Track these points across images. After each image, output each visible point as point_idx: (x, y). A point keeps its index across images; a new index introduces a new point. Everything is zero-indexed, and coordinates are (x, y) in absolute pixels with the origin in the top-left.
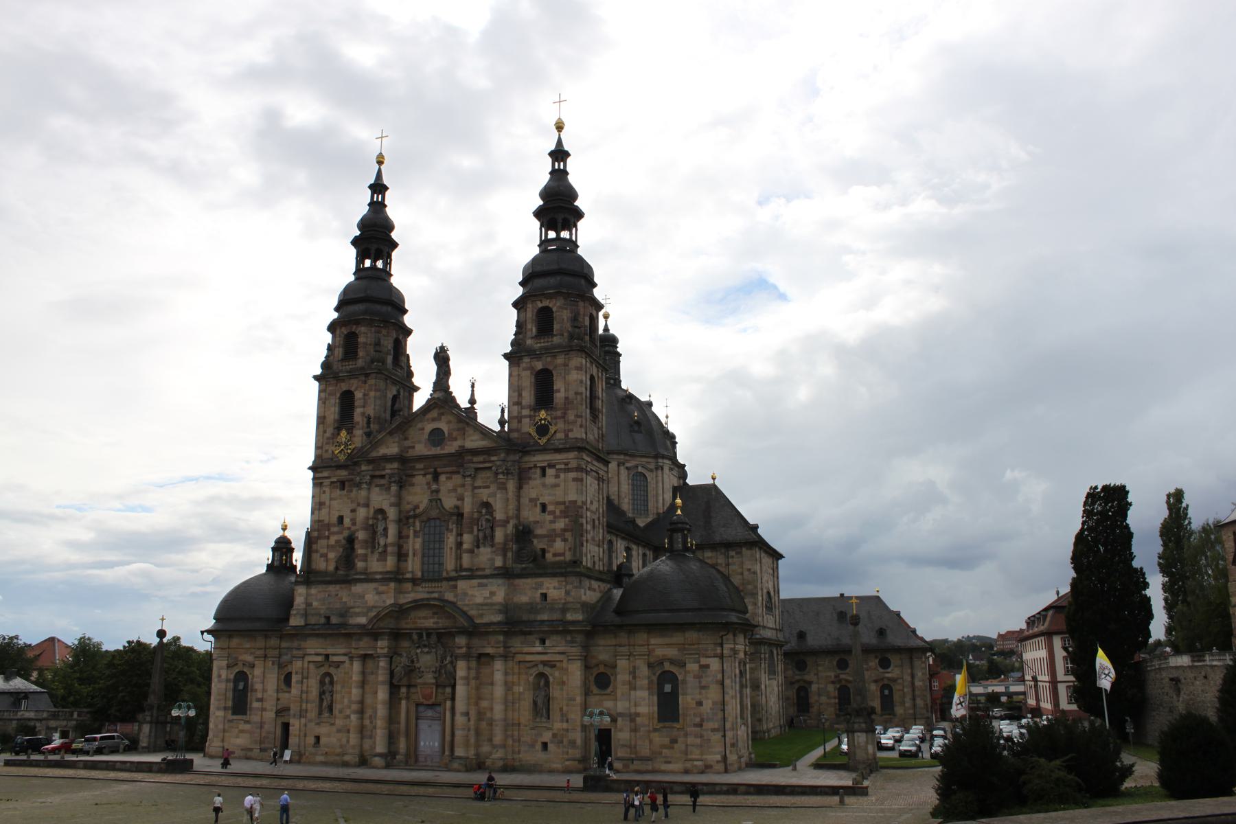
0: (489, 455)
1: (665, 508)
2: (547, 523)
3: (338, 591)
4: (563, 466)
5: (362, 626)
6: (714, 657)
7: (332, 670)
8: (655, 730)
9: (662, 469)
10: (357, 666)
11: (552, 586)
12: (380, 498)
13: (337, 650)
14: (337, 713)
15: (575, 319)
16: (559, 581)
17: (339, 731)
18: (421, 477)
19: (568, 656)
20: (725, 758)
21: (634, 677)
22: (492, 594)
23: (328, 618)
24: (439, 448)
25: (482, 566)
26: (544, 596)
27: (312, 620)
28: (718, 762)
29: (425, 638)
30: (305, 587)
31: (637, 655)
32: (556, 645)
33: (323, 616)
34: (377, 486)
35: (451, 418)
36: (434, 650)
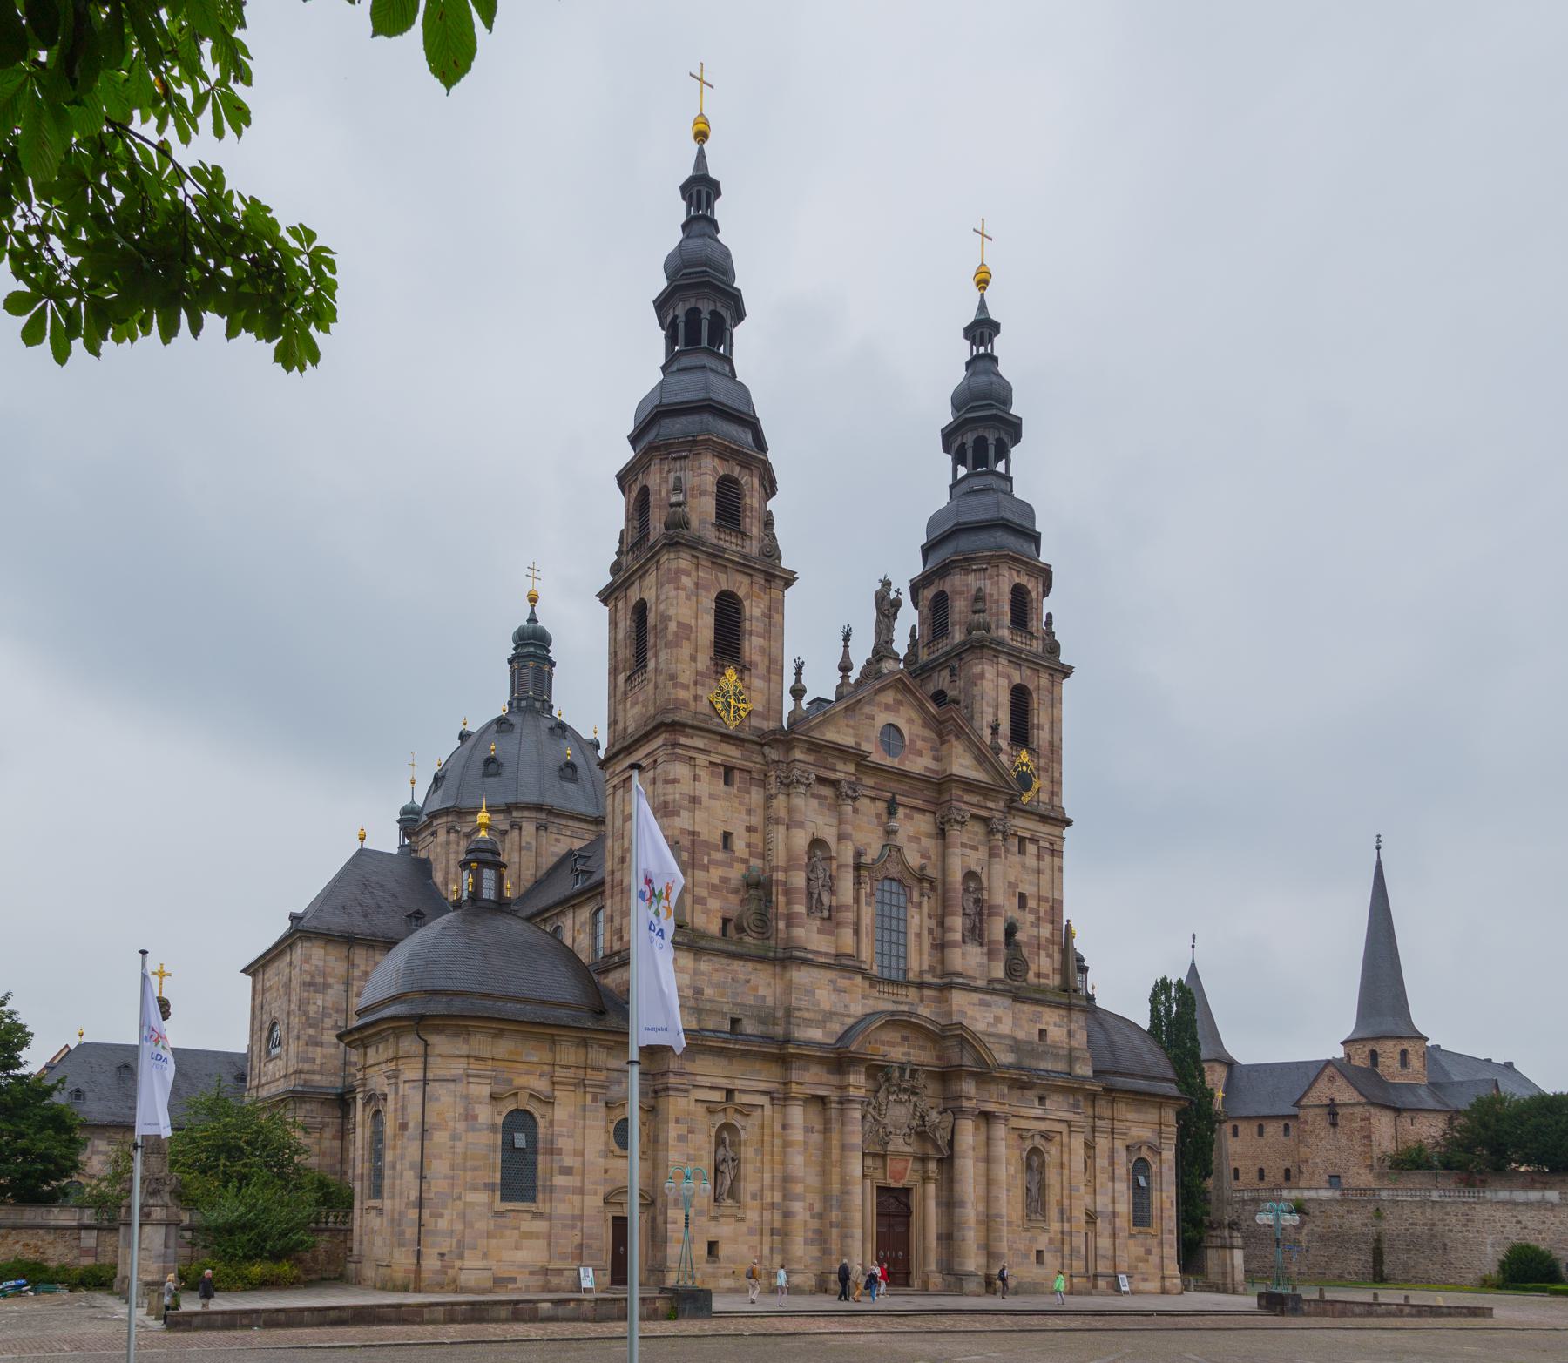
0: (985, 797)
2: (1028, 924)
3: (750, 973)
4: (1047, 845)
5: (821, 1045)
7: (737, 1120)
8: (1132, 1236)
10: (797, 1114)
11: (1051, 1021)
12: (820, 820)
13: (754, 1081)
14: (748, 1198)
16: (1059, 1015)
17: (751, 1232)
18: (867, 801)
19: (1070, 1126)
21: (1112, 1163)
22: (998, 1019)
23: (735, 1022)
24: (896, 760)
25: (971, 973)
26: (1042, 1033)
27: (710, 1023)
29: (907, 1077)
30: (692, 955)
31: (1118, 1133)
32: (1058, 1108)
33: (729, 1016)
34: (814, 796)
35: (914, 715)
36: (914, 1099)
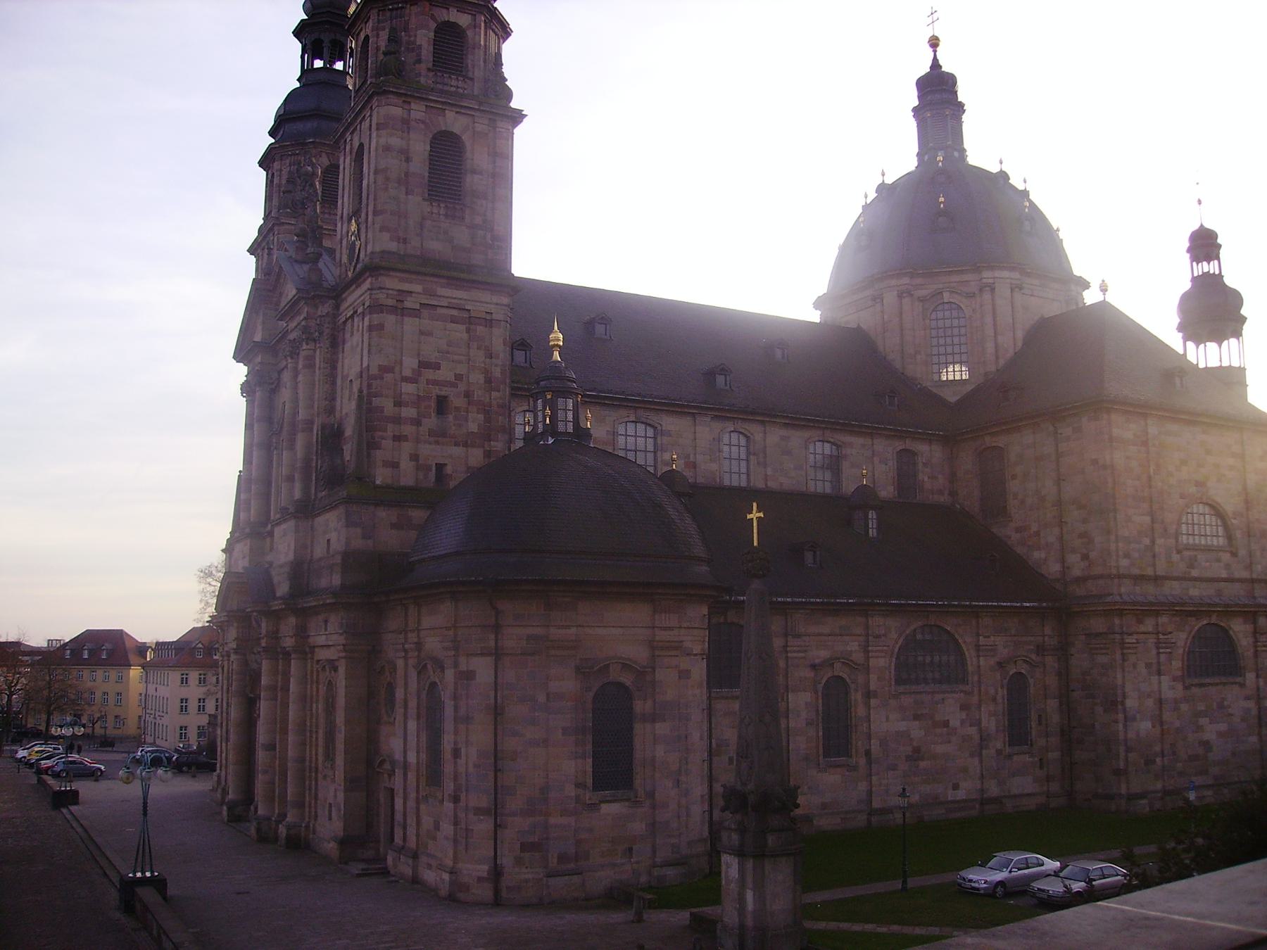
1: (1002, 362)
6: (482, 654)
9: (993, 290)
15: (393, 39)
20: (497, 873)
28: (480, 879)
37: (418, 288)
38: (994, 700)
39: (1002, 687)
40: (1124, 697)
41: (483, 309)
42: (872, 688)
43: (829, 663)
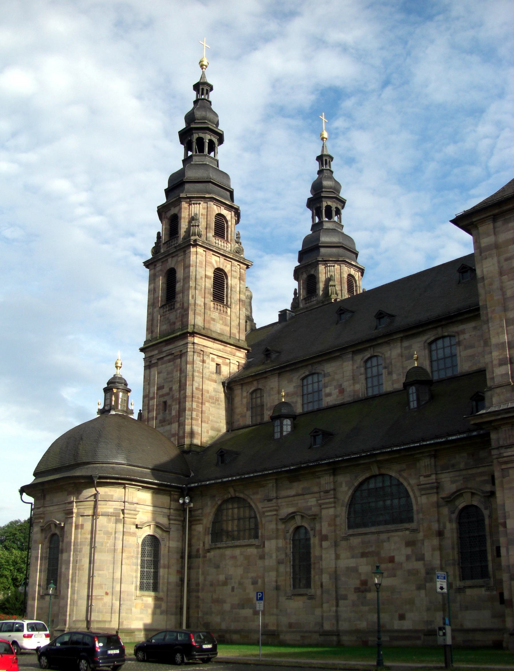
37: (156, 352)
38: (440, 534)
39: (450, 521)
40: (505, 517)
41: (178, 350)
42: (324, 532)
43: (291, 517)
